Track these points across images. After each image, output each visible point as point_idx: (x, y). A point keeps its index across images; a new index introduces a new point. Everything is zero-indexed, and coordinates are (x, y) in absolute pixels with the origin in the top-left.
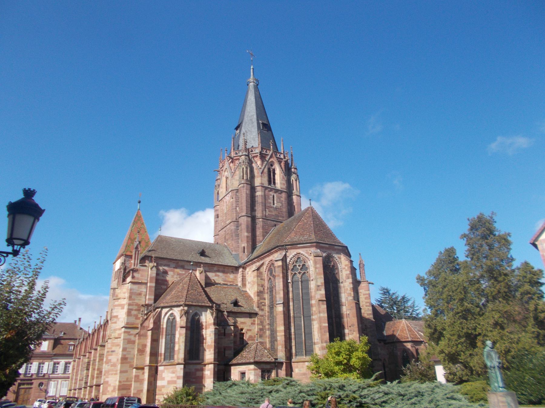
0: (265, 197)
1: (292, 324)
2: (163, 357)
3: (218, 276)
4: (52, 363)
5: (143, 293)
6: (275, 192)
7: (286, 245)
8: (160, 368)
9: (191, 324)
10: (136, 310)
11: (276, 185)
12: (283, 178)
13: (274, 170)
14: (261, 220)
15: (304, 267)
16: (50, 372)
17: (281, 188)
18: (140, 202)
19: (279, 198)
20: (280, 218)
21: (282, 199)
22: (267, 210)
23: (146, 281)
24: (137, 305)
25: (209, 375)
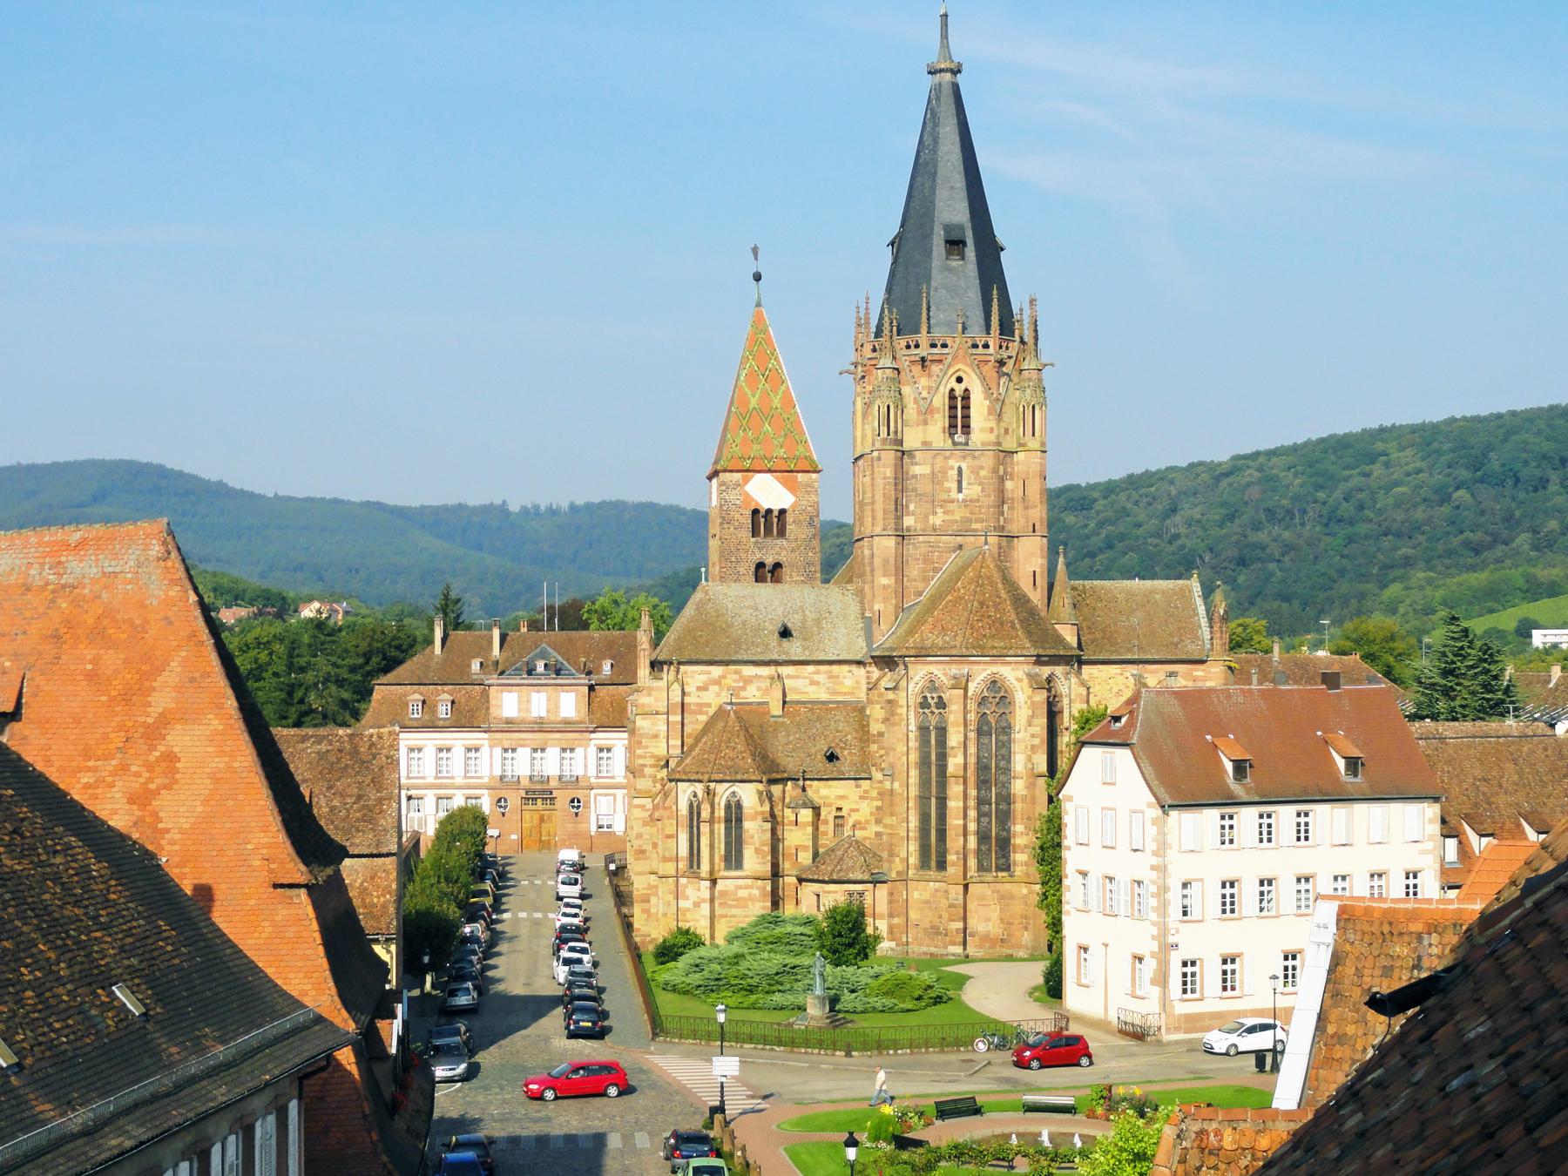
0: (936, 478)
3: (816, 683)
4: (592, 750)
5: (663, 734)
11: (972, 436)
12: (990, 413)
15: (941, 704)
16: (592, 772)
17: (983, 444)
18: (757, 277)
19: (975, 471)
20: (974, 526)
21: (983, 473)
22: (939, 510)
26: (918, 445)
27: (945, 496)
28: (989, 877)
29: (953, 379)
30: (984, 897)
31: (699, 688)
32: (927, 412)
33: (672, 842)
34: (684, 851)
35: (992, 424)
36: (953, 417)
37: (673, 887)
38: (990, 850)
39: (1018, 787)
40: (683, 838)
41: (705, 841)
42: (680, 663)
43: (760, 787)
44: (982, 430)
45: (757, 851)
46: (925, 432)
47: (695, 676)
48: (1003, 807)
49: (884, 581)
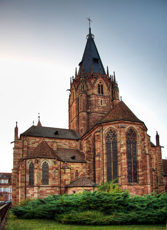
1: (105, 167)
2: (28, 183)
5: (21, 154)
6: (102, 98)
7: (102, 123)
8: (28, 188)
9: (43, 168)
10: (17, 162)
12: (108, 90)
13: (102, 85)
14: (93, 113)
17: (106, 96)
19: (105, 101)
21: (107, 102)
22: (97, 108)
23: (22, 148)
24: (18, 159)
25: (54, 192)
26: (92, 94)
27: (98, 105)
28: (132, 184)
29: (99, 82)
30: (131, 190)
31: (32, 143)
32: (93, 87)
33: (24, 177)
34: (28, 180)
35: (109, 92)
36: (99, 90)
37: (24, 190)
38: (131, 176)
39: (139, 158)
40: (28, 176)
41: (35, 175)
42: (27, 136)
43: (55, 160)
44: (106, 93)
45: (54, 179)
46: (93, 91)
47: (32, 140)
48: (135, 164)
49: (83, 122)
